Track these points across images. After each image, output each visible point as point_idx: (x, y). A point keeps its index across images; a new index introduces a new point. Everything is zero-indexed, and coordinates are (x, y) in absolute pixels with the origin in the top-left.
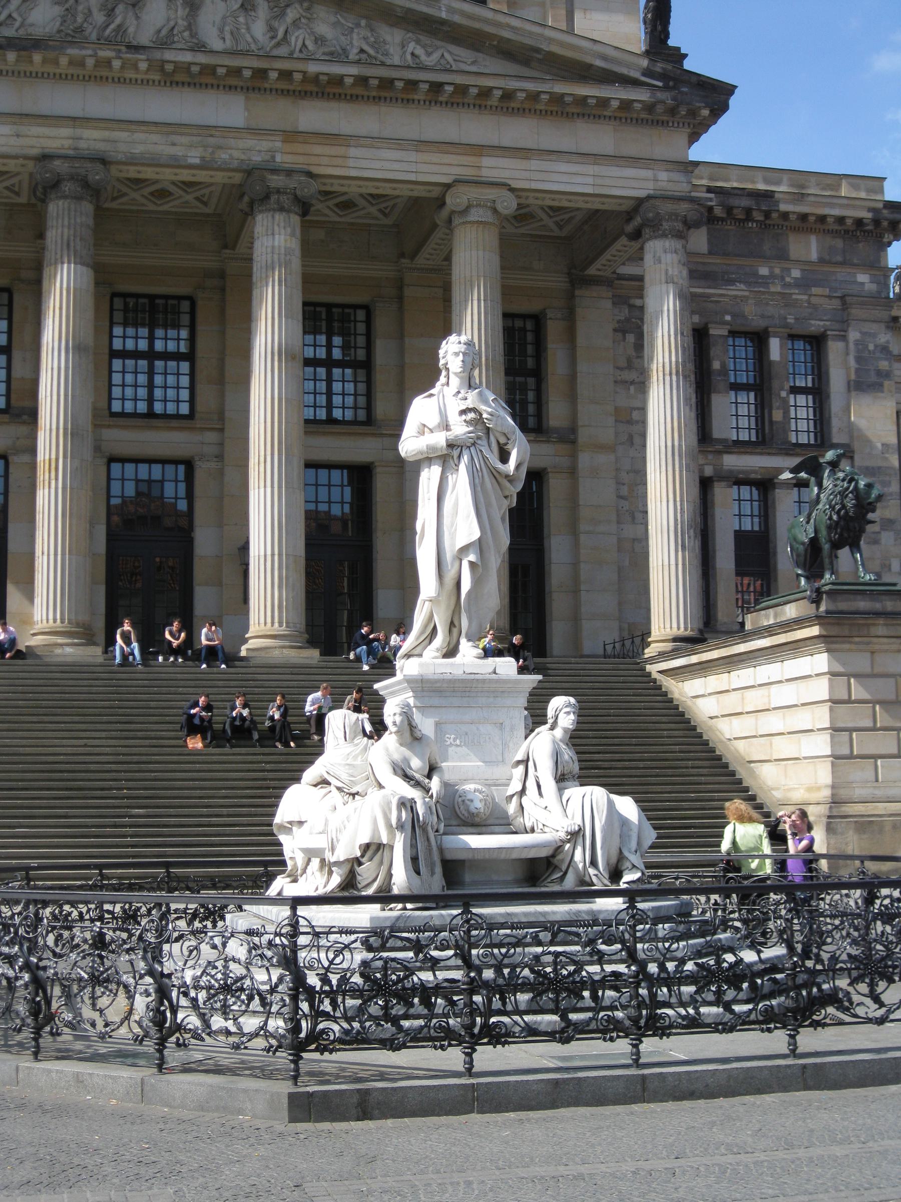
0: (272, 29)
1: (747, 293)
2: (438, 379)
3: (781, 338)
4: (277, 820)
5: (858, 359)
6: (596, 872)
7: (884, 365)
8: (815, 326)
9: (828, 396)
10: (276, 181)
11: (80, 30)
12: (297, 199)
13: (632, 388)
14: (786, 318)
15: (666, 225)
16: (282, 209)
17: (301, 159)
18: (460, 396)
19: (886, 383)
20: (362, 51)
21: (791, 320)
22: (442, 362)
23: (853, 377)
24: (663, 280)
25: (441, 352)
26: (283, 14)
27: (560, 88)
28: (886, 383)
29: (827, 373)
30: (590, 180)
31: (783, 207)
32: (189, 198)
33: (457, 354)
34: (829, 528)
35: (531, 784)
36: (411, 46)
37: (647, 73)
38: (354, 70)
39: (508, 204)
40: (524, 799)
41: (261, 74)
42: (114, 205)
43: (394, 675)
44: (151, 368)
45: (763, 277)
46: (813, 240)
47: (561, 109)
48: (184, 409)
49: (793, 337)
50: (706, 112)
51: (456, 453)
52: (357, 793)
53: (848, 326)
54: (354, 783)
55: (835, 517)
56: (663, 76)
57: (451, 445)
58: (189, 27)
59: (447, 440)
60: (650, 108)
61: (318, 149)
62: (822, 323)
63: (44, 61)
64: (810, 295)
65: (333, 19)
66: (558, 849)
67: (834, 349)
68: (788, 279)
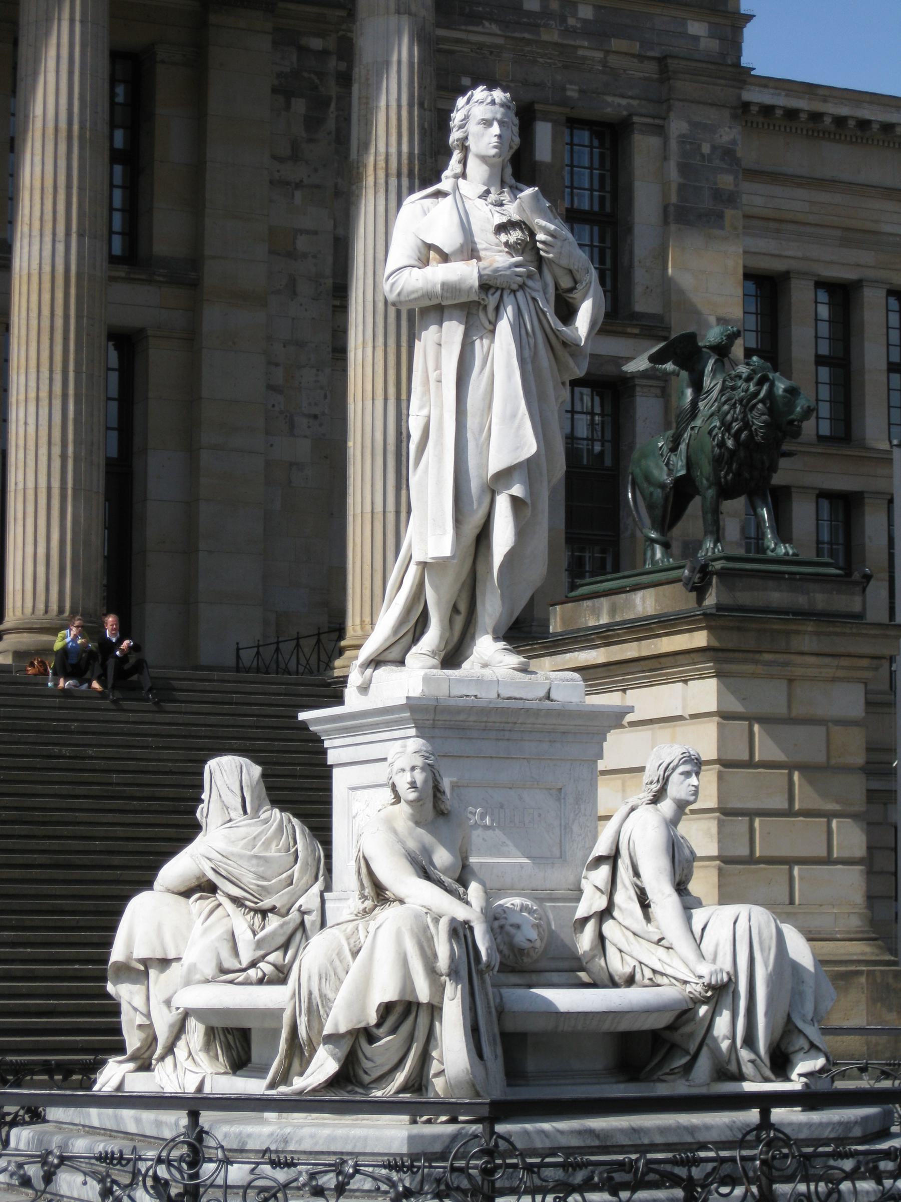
1: (500, 41)
2: (445, 166)
3: (555, 123)
4: (117, 954)
5: (684, 169)
6: (753, 1056)
7: (726, 181)
8: (614, 105)
9: (629, 230)
13: (298, 194)
14: (564, 89)
18: (493, 197)
19: (729, 213)
21: (572, 92)
22: (455, 136)
23: (674, 199)
24: (392, 7)
25: (457, 117)
28: (729, 213)
33: (487, 123)
34: (717, 461)
35: (625, 898)
40: (609, 928)
45: (530, 14)
49: (573, 123)
52: (273, 910)
53: (669, 109)
55: (730, 443)
57: (485, 286)
59: (480, 277)
62: (624, 102)
64: (607, 52)
66: (684, 1014)
67: (643, 149)
68: (571, 21)
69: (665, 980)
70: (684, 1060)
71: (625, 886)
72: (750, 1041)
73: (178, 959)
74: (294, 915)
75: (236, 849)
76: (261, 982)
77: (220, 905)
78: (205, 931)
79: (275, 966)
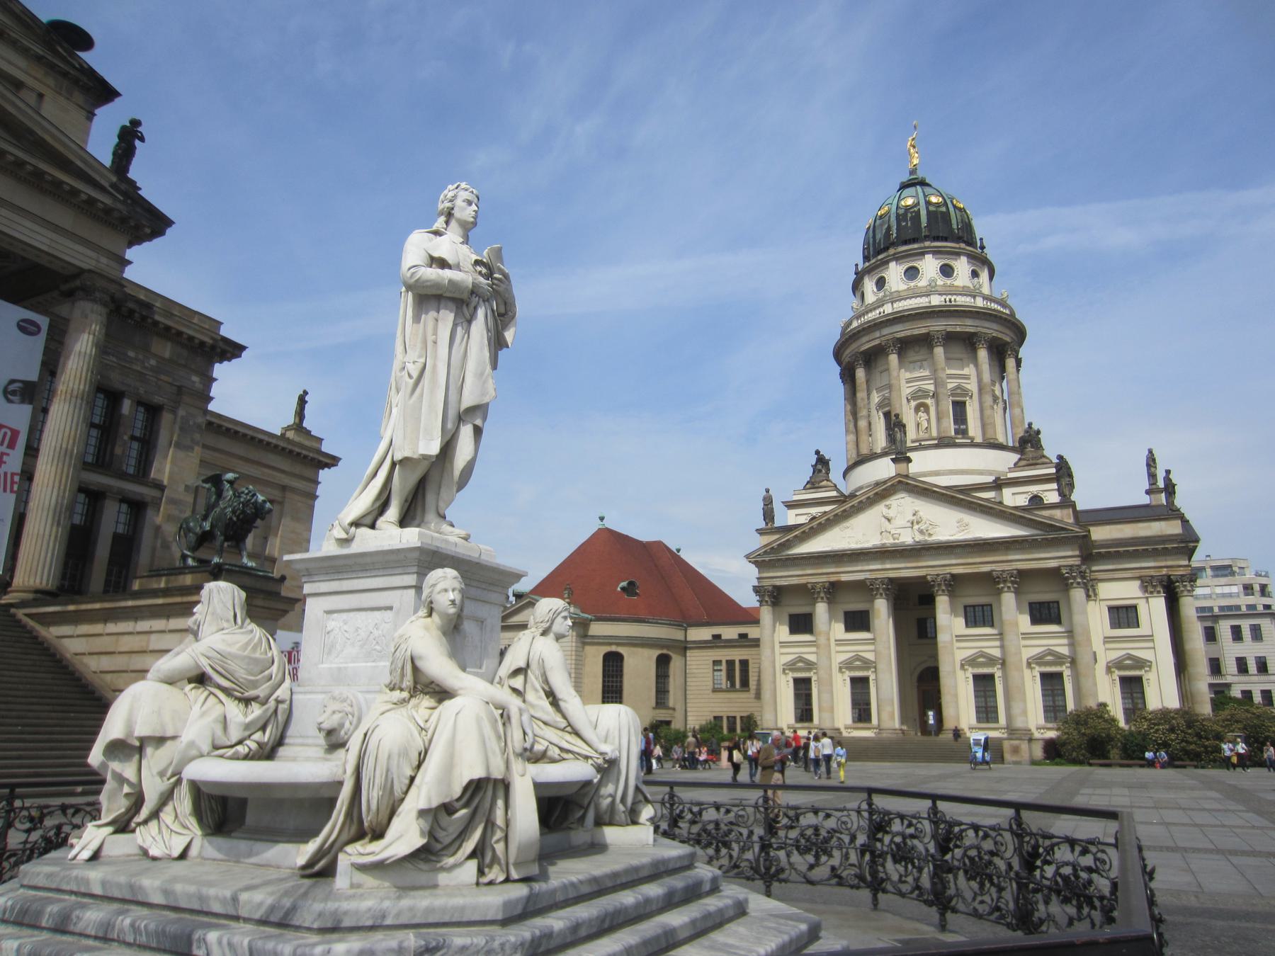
8: (157, 399)
15: (97, 294)
21: (142, 391)
27: (43, 166)
29: (158, 432)
30: (48, 242)
31: (157, 317)
34: (227, 526)
37: (113, 185)
43: (307, 550)
46: (169, 345)
49: (139, 403)
50: (148, 231)
51: (475, 300)
52: (255, 699)
54: (255, 685)
56: (125, 194)
57: (472, 292)
60: (108, 211)
67: (166, 418)
69: (570, 756)
70: (581, 813)
71: (536, 690)
72: (623, 800)
73: (174, 738)
74: (272, 703)
75: (234, 650)
76: (247, 757)
77: (211, 693)
78: (203, 715)
79: (258, 743)
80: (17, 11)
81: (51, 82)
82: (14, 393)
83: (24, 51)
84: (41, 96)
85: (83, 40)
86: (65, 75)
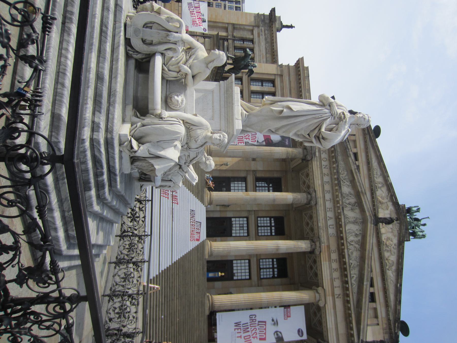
0: (352, 241)
10: (318, 244)
11: (344, 198)
12: (314, 250)
16: (311, 246)
17: (324, 250)
20: (352, 264)
26: (357, 244)
27: (353, 315)
30: (331, 327)
32: (308, 230)
36: (354, 276)
38: (347, 261)
39: (321, 304)
41: (342, 238)
42: (303, 215)
44: (268, 226)
47: (347, 317)
48: (260, 234)
51: (328, 107)
58: (349, 222)
61: (327, 254)
63: (336, 190)
65: (358, 256)
80: (398, 308)
81: (385, 326)
82: (277, 335)
83: (388, 314)
84: (378, 324)
85: (406, 332)
86: (390, 329)
